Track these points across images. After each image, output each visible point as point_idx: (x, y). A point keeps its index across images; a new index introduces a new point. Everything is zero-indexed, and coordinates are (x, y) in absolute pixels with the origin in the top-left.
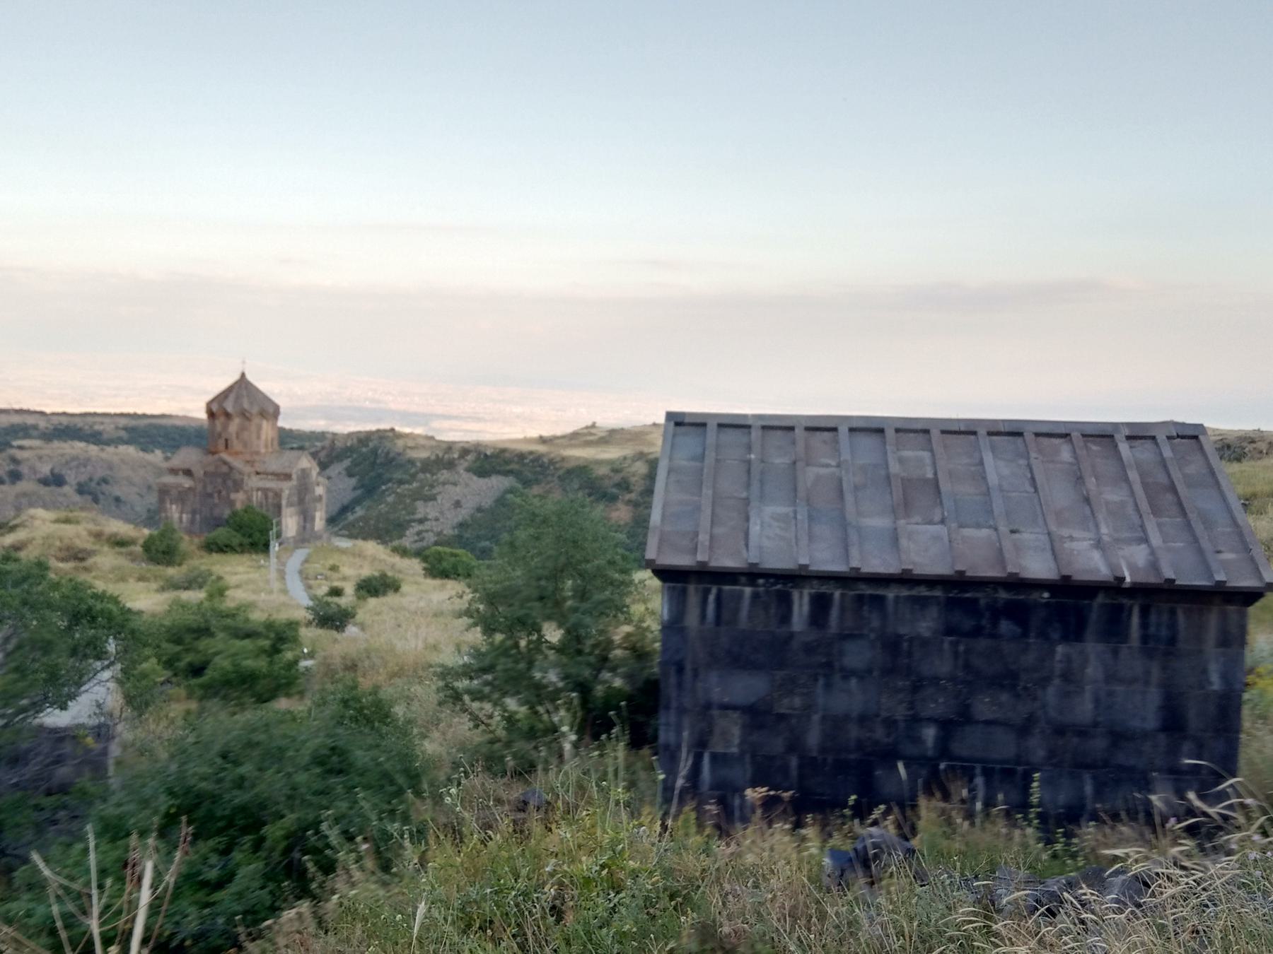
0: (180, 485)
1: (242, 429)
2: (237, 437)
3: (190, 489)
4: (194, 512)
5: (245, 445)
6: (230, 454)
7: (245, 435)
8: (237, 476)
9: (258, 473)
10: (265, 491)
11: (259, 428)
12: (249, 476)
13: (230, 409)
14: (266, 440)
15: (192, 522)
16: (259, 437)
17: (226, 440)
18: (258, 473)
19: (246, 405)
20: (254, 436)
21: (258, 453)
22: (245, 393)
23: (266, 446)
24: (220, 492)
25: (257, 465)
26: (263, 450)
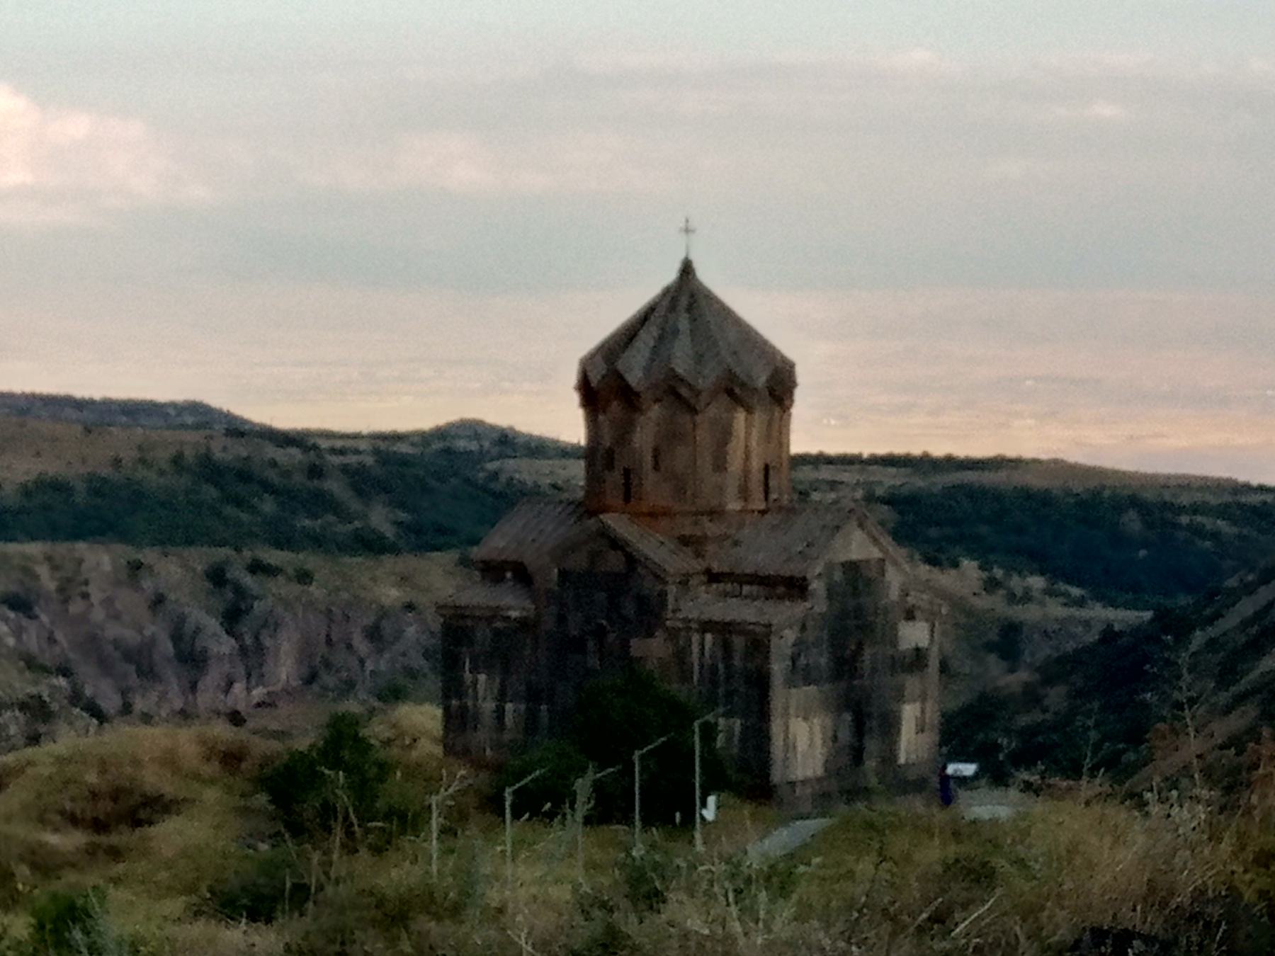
0: (495, 613)
1: (671, 437)
2: (656, 467)
3: (523, 624)
4: (533, 696)
5: (680, 490)
6: (636, 516)
7: (680, 457)
8: (649, 586)
9: (713, 577)
10: (724, 630)
11: (725, 435)
12: (684, 583)
13: (635, 377)
14: (746, 473)
15: (530, 724)
16: (720, 465)
17: (627, 473)
18: (713, 577)
19: (682, 365)
20: (705, 463)
21: (715, 513)
22: (684, 323)
23: (744, 493)
24: (600, 633)
25: (711, 548)
26: (734, 505)
